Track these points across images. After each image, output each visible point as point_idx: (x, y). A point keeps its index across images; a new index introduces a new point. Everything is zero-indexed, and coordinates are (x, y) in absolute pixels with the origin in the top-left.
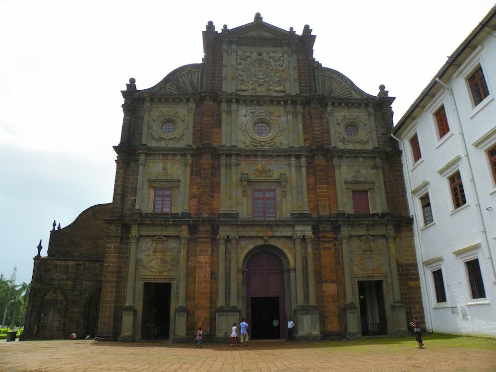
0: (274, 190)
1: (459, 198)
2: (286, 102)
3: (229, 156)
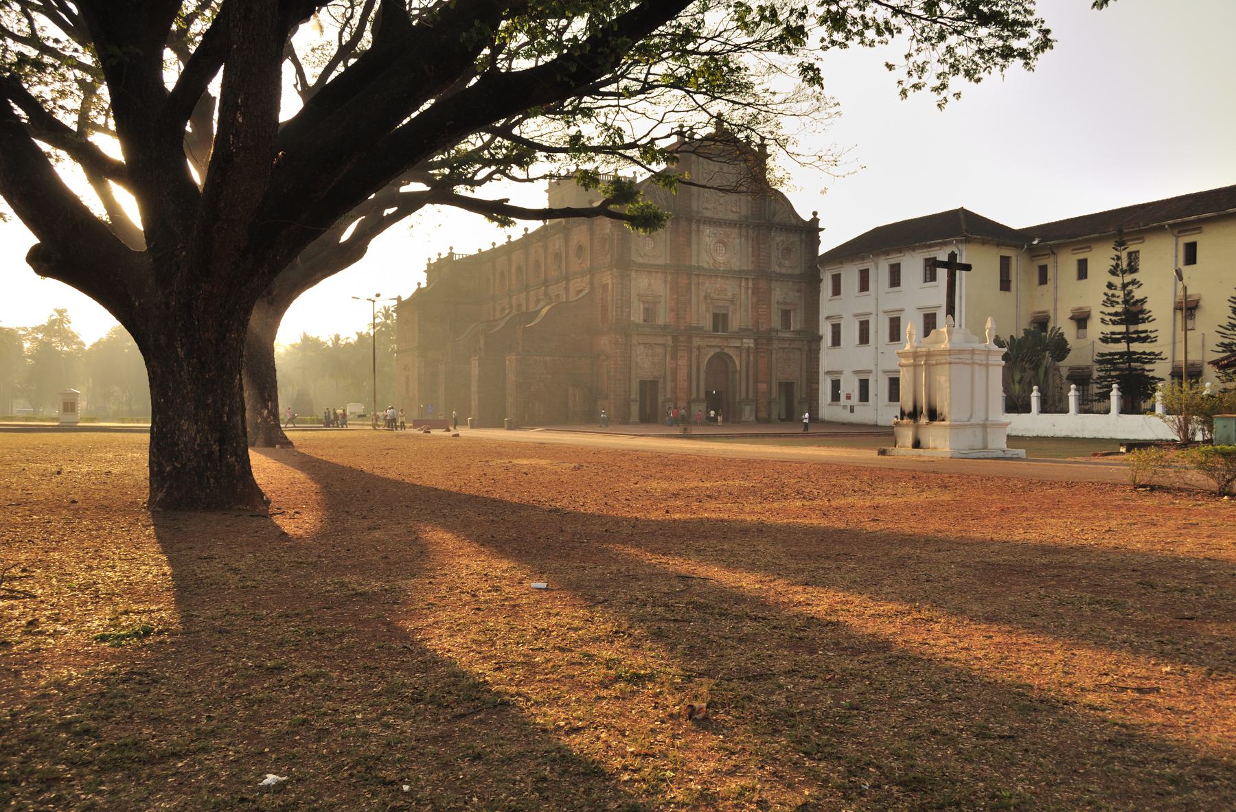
0: (728, 307)
1: (864, 338)
2: (741, 225)
3: (698, 275)
